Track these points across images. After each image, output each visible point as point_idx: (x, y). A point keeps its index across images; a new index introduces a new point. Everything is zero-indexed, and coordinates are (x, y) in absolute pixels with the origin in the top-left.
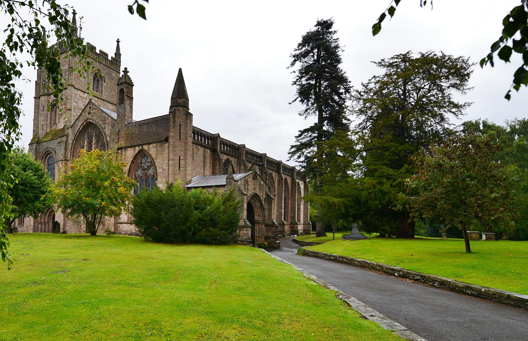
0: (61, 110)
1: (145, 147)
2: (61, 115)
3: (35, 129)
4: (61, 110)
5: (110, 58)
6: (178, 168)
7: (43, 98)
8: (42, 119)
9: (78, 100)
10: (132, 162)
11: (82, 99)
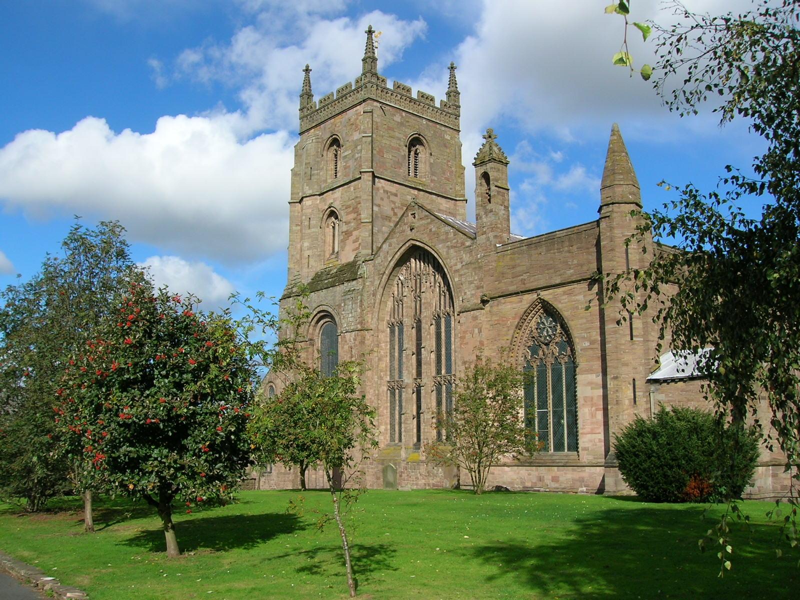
0: (347, 223)
1: (546, 295)
2: (348, 234)
3: (292, 266)
4: (347, 223)
5: (438, 105)
6: (629, 338)
7: (307, 202)
8: (306, 244)
9: (382, 199)
10: (519, 327)
11: (389, 198)
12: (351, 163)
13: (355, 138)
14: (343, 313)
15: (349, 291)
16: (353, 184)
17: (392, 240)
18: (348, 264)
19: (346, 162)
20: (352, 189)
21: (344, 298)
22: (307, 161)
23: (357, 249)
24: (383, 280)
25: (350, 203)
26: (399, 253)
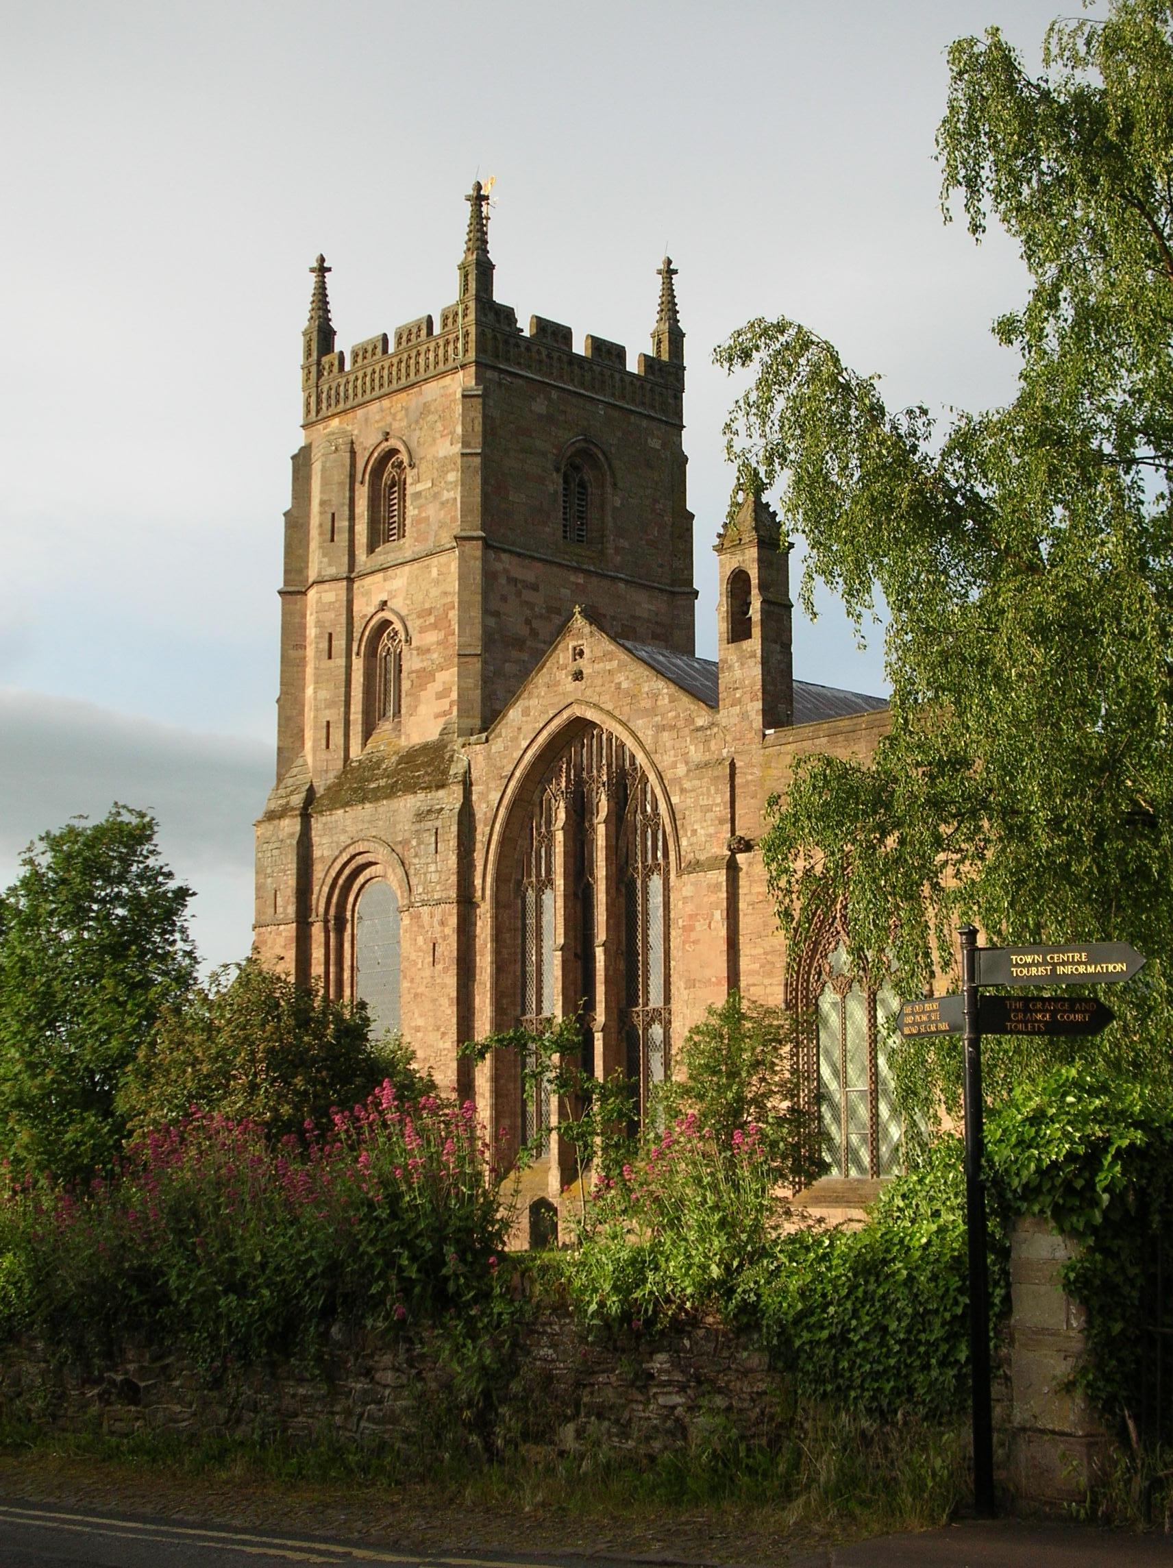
4: (423, 651)
12: (431, 511)
13: (441, 454)
14: (416, 861)
15: (429, 811)
16: (435, 561)
17: (531, 702)
18: (425, 748)
19: (420, 507)
20: (434, 572)
21: (417, 827)
22: (326, 498)
23: (445, 714)
24: (509, 791)
25: (427, 606)
26: (545, 733)
